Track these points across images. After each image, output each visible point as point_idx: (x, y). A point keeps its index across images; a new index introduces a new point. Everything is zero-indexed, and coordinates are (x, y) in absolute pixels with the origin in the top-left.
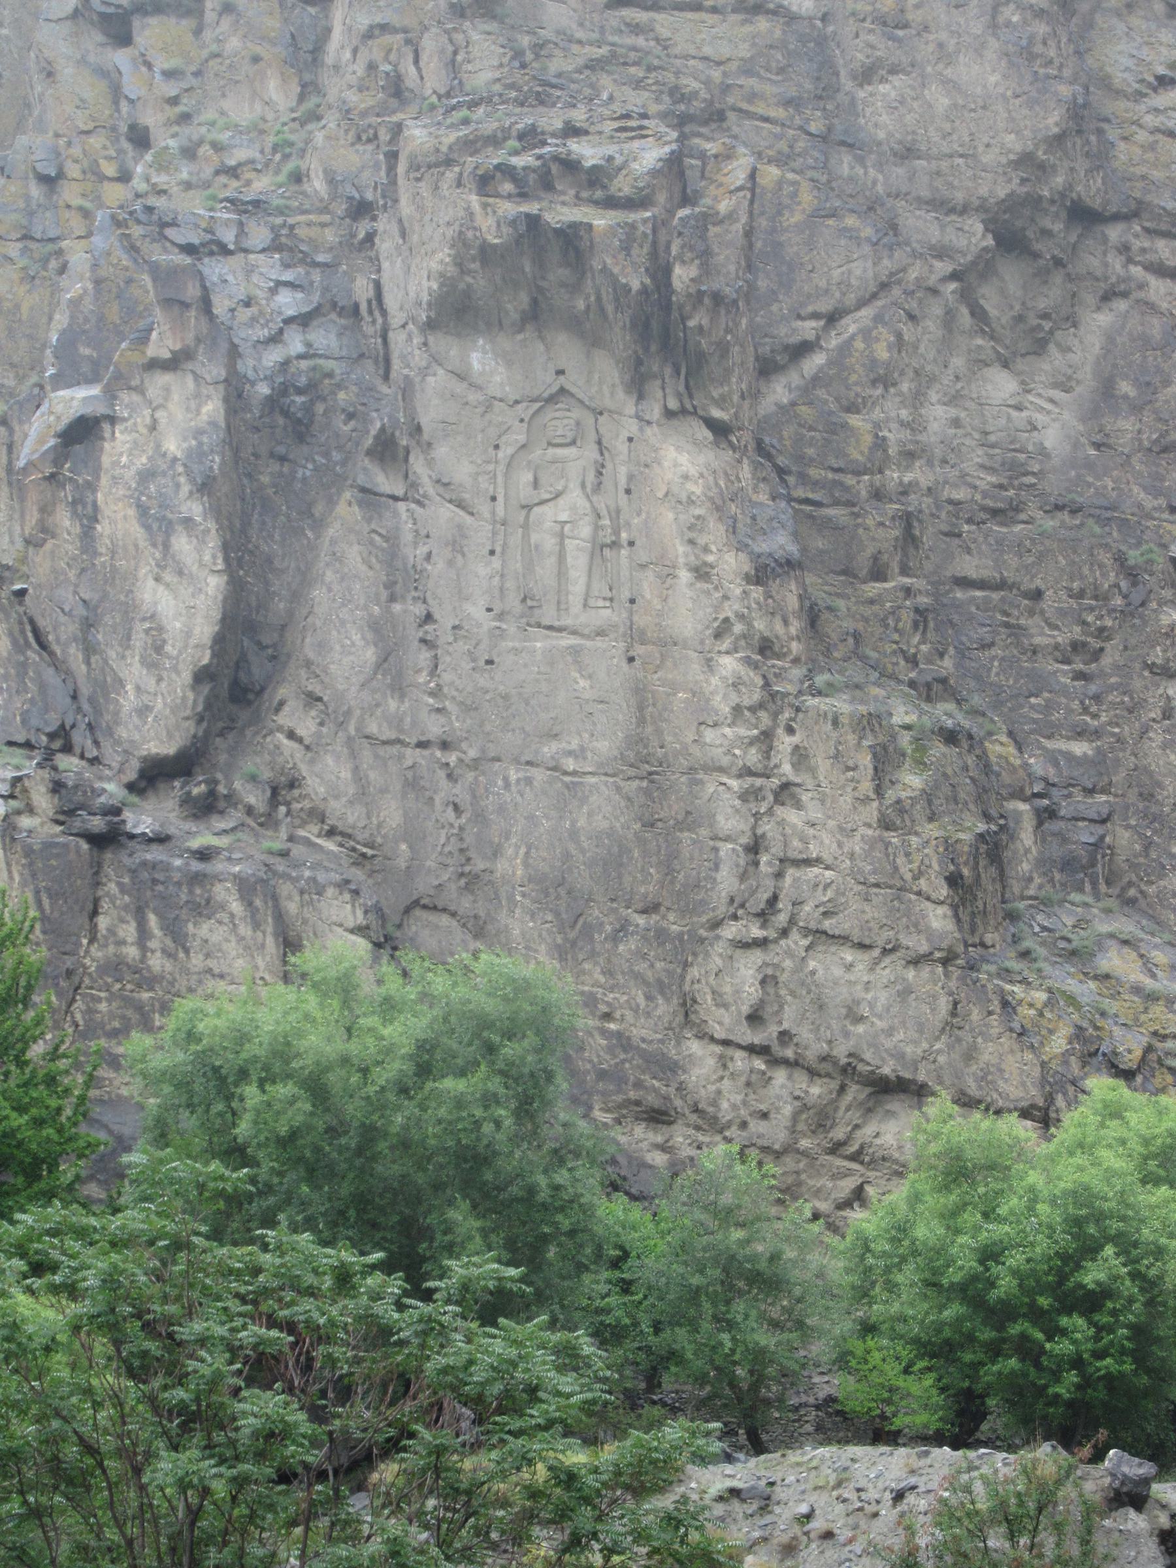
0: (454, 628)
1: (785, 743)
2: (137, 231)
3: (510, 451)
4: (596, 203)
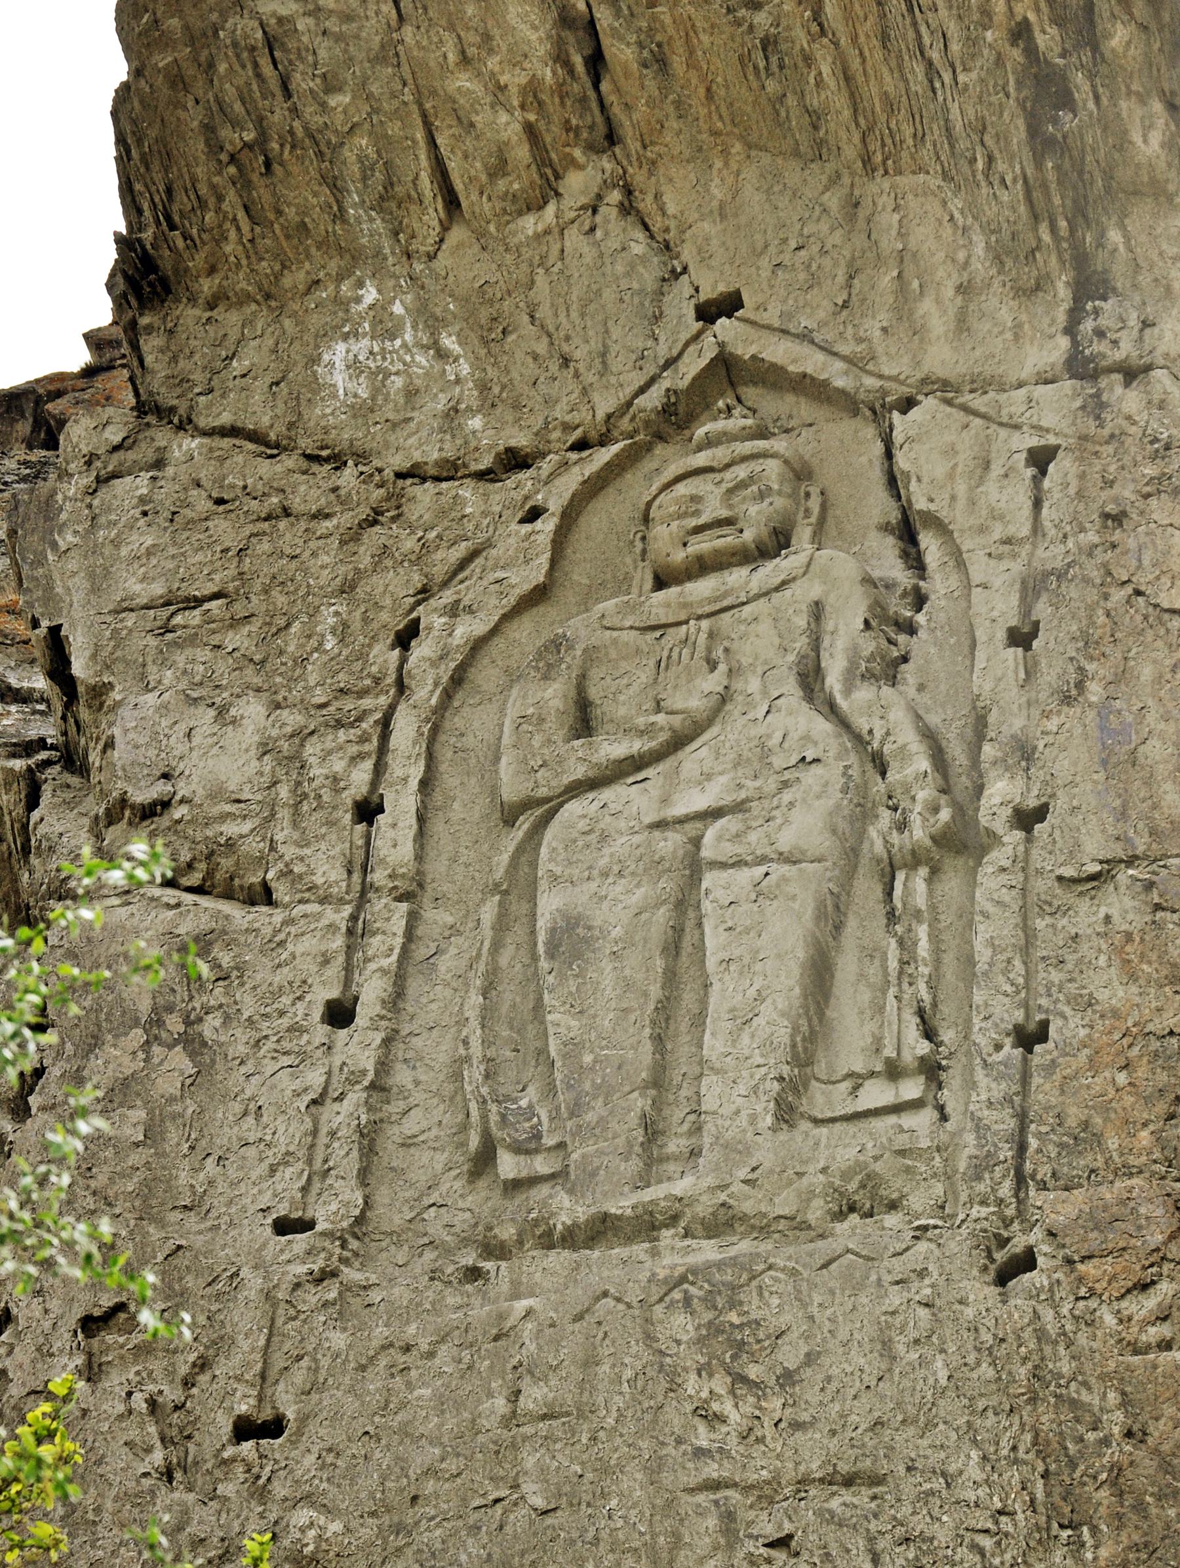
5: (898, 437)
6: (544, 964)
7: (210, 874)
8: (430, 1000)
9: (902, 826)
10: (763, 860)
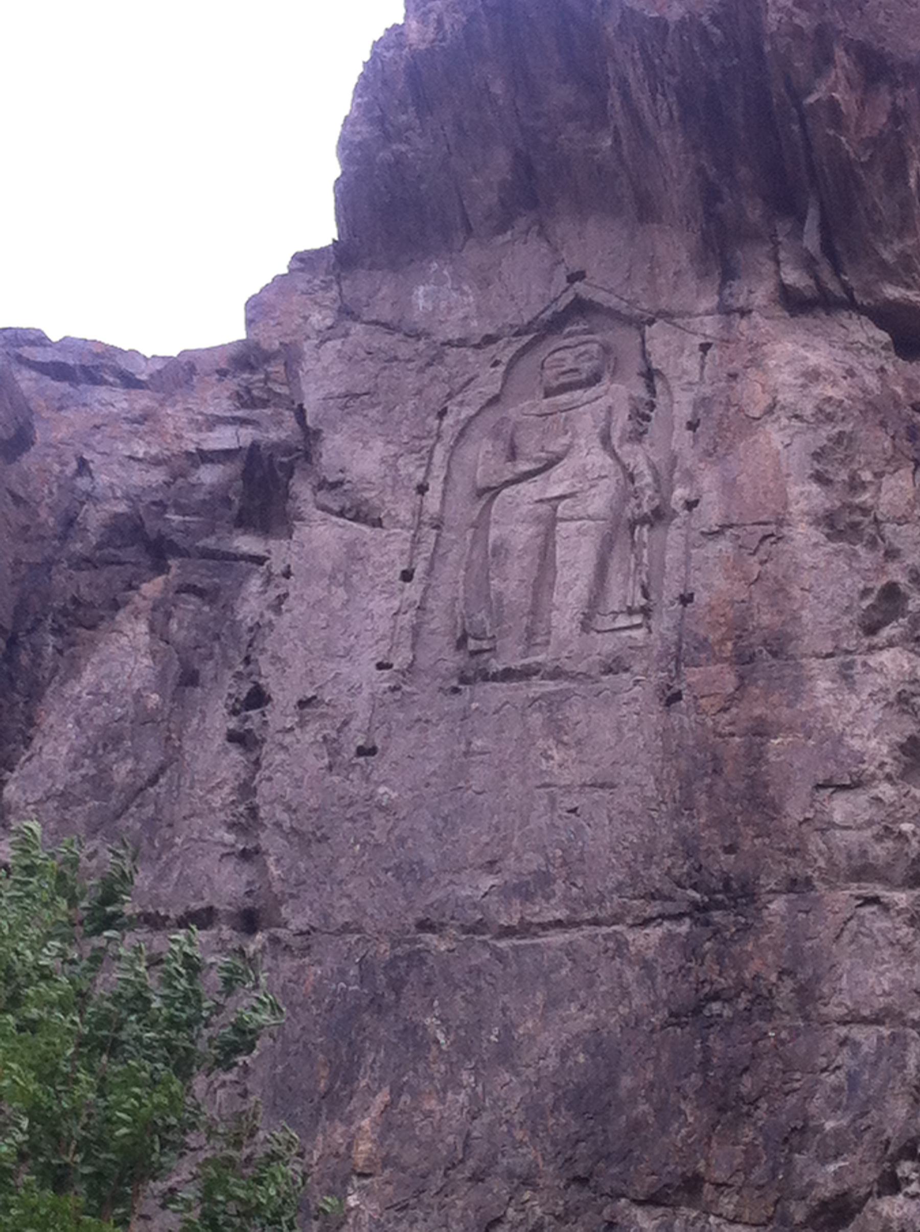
0: (303, 704)
5: (647, 336)
6: (490, 558)
7: (358, 513)
9: (639, 506)
10: (581, 519)
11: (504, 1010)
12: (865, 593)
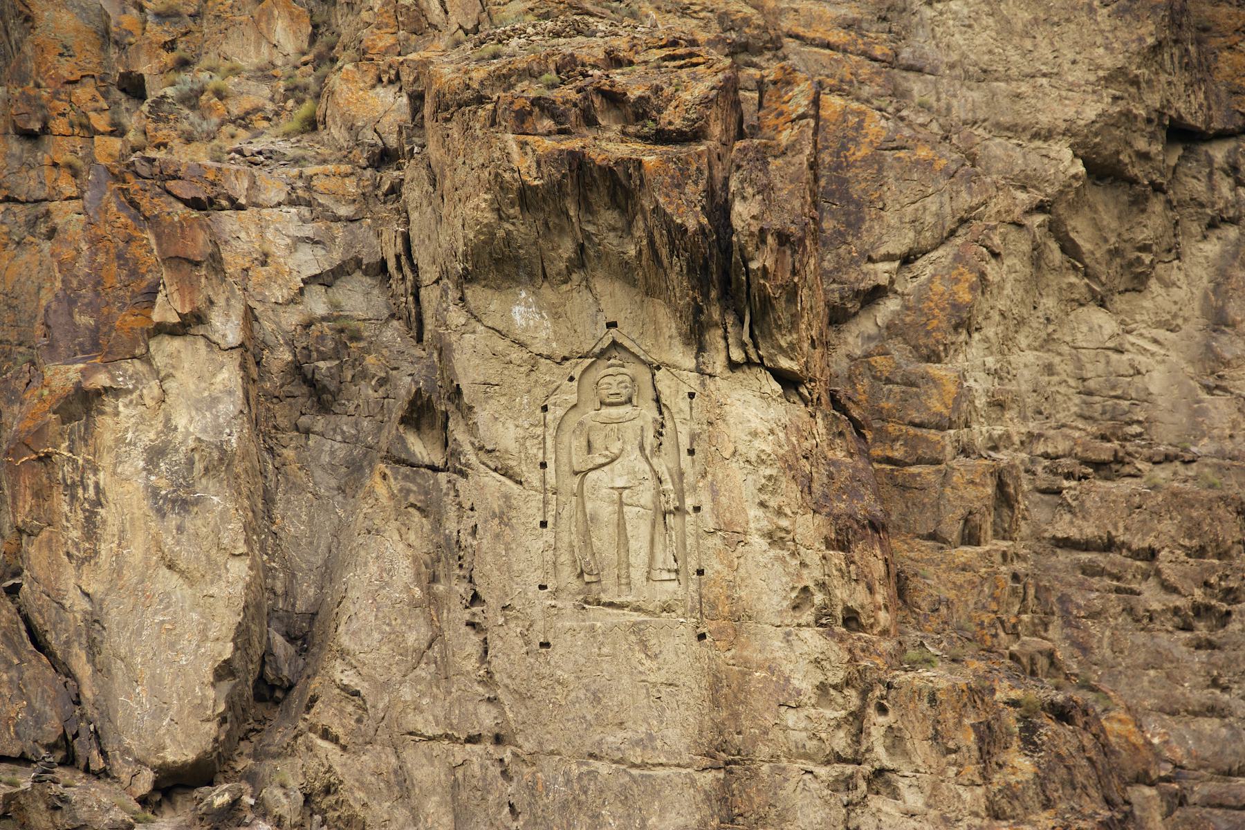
1: (877, 724)
2: (134, 185)
3: (560, 412)
4: (644, 138)
8: (564, 524)
11: (640, 809)
12: (793, 588)
